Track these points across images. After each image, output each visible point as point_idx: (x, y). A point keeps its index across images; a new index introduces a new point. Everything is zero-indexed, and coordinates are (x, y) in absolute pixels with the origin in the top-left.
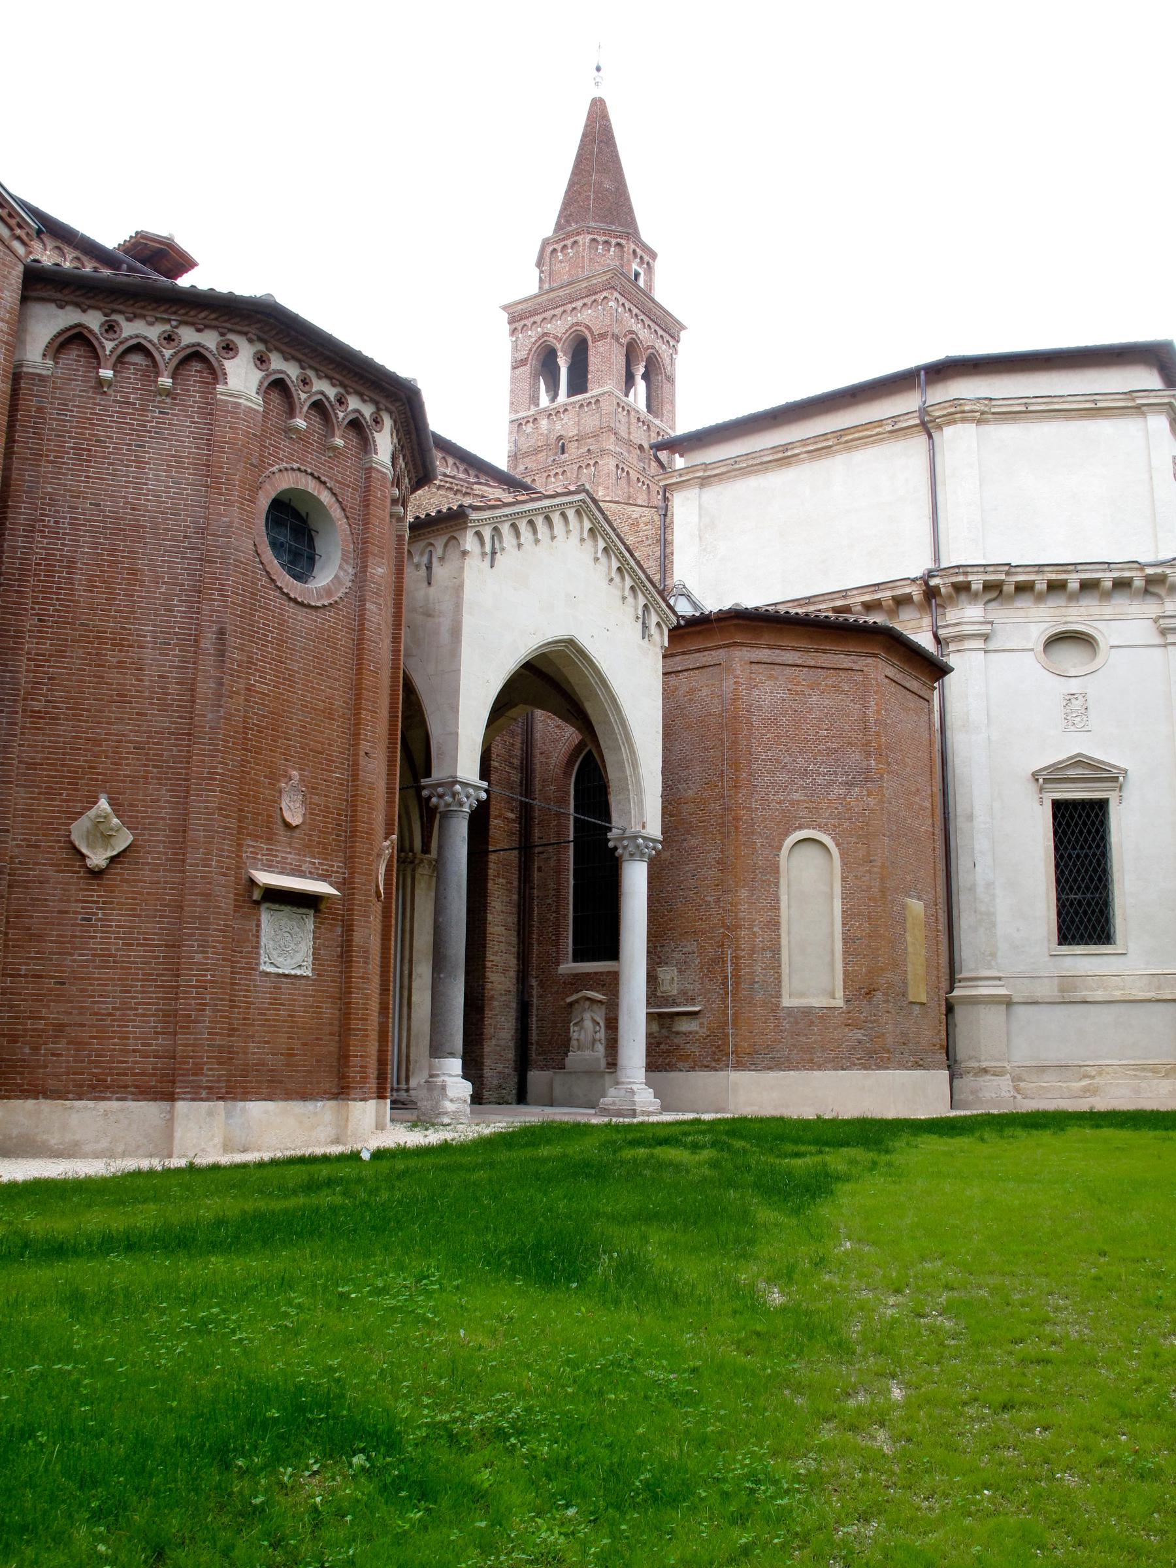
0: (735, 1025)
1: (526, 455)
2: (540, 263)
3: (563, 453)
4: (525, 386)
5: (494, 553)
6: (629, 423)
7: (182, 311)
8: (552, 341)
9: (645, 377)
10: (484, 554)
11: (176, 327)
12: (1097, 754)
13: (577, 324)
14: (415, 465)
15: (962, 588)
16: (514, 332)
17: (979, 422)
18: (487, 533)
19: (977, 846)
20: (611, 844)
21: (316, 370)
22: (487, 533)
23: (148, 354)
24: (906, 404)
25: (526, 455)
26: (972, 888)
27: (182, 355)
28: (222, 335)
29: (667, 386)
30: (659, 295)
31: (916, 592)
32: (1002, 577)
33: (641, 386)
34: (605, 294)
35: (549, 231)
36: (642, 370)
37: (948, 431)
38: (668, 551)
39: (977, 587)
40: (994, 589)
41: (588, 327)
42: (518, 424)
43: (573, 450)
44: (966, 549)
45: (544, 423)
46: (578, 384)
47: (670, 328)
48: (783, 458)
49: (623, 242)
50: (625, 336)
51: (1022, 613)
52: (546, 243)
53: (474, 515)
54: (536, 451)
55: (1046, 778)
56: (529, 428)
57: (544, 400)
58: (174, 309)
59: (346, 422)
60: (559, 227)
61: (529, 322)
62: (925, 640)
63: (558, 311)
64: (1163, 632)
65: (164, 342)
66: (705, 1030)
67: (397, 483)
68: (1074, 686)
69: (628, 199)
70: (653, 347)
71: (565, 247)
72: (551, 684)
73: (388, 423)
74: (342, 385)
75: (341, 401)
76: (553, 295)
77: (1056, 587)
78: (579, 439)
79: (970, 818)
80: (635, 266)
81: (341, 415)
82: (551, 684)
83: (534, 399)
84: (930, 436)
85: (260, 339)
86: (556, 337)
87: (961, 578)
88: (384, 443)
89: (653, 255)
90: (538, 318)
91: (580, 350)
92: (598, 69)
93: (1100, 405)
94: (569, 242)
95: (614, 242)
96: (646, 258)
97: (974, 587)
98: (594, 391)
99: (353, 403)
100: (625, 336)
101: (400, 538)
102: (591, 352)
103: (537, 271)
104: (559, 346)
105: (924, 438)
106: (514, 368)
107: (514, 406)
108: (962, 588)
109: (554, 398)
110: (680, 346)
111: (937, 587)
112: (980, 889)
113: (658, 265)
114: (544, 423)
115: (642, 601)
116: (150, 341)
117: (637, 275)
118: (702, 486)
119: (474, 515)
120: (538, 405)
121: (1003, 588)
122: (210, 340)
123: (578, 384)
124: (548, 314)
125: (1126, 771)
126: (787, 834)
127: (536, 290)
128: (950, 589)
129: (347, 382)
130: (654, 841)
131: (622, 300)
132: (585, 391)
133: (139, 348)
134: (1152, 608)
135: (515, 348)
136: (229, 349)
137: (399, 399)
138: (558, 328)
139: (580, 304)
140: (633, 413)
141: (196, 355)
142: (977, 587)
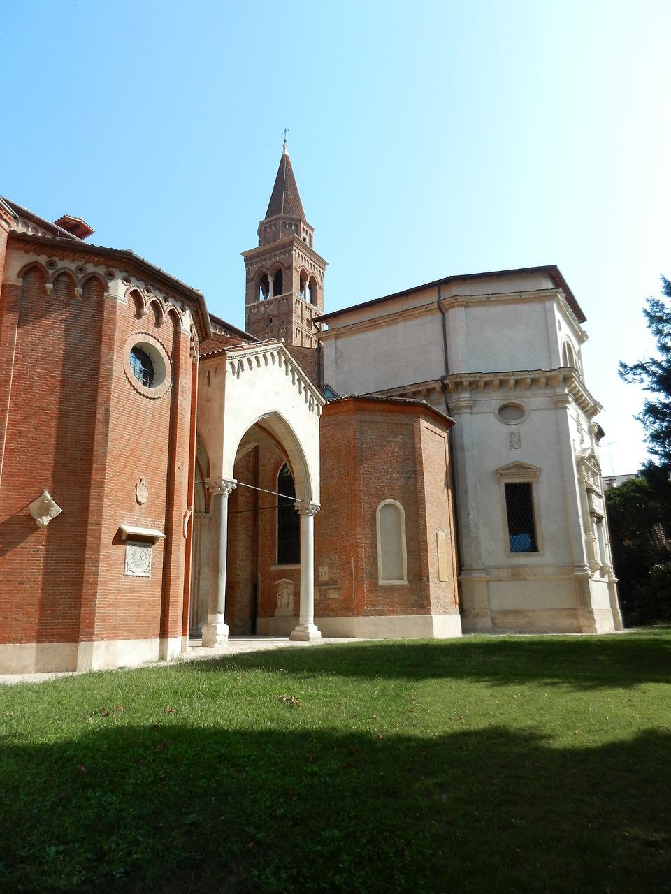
0: (356, 593)
1: (254, 323)
2: (259, 233)
3: (271, 322)
4: (253, 291)
5: (239, 372)
7: (87, 257)
8: (265, 271)
10: (233, 373)
11: (85, 264)
12: (526, 461)
14: (201, 331)
15: (458, 385)
16: (246, 266)
17: (466, 307)
18: (236, 362)
19: (470, 506)
20: (296, 509)
21: (153, 286)
22: (236, 362)
23: (69, 276)
24: (431, 298)
25: (254, 323)
26: (468, 526)
27: (87, 277)
28: (107, 268)
29: (319, 291)
30: (314, 248)
31: (438, 386)
32: (478, 379)
33: (307, 291)
34: (290, 248)
35: (262, 217)
36: (308, 284)
37: (451, 311)
38: (321, 368)
39: (466, 383)
40: (473, 386)
41: (282, 264)
42: (249, 310)
43: (276, 321)
44: (463, 365)
45: (262, 308)
46: (278, 290)
47: (322, 263)
48: (374, 324)
49: (298, 223)
50: (300, 267)
51: (488, 395)
52: (262, 224)
53: (229, 354)
54: (258, 322)
55: (499, 473)
56: (255, 311)
57: (262, 298)
58: (83, 256)
59: (168, 311)
60: (267, 216)
62: (441, 410)
64: (555, 403)
65: (79, 271)
66: (342, 596)
67: (192, 339)
68: (514, 428)
69: (300, 203)
70: (313, 273)
71: (270, 226)
73: (188, 312)
74: (166, 293)
77: (503, 383)
78: (279, 316)
79: (466, 492)
80: (303, 235)
81: (165, 307)
83: (258, 297)
84: (443, 313)
85: (126, 271)
86: (267, 268)
87: (458, 380)
88: (187, 319)
89: (312, 229)
90: (259, 259)
92: (285, 141)
93: (523, 297)
94: (273, 223)
95: (293, 223)
96: (309, 231)
97: (465, 383)
100: (300, 267)
101: (194, 365)
102: (284, 275)
103: (258, 236)
104: (268, 272)
105: (439, 315)
106: (247, 282)
107: (247, 302)
108: (458, 385)
109: (266, 298)
110: (325, 273)
111: (448, 385)
112: (472, 526)
113: (314, 235)
114: (262, 308)
115: (309, 394)
116: (72, 271)
117: (305, 239)
118: (336, 338)
119: (229, 354)
120: (259, 300)
121: (479, 384)
122: (101, 270)
123: (278, 290)
124: (263, 257)
125: (540, 469)
126: (379, 502)
128: (453, 386)
129: (168, 292)
130: (317, 506)
131: (298, 251)
132: (281, 294)
133: (64, 274)
134: (549, 391)
135: (248, 273)
136: (111, 276)
137: (193, 300)
138: (268, 263)
139: (278, 252)
140: (303, 304)
141: (94, 277)
142: (466, 383)
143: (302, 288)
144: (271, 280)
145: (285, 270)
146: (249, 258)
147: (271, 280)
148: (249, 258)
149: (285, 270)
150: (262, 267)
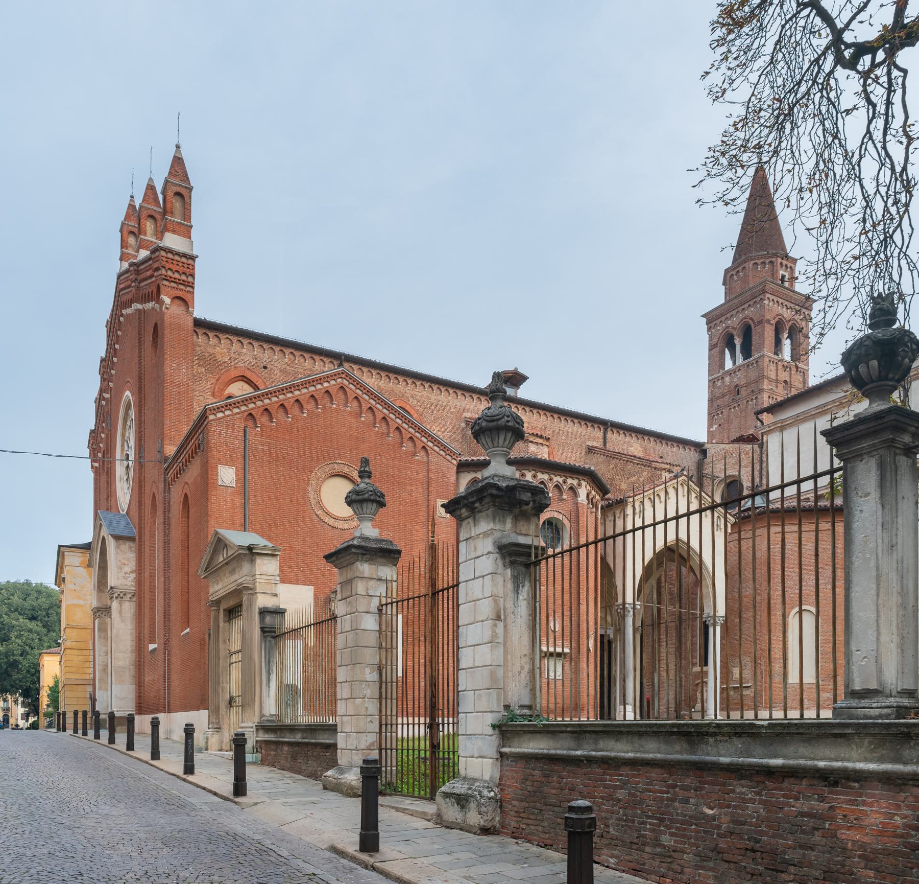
6: (777, 370)
9: (789, 337)
13: (745, 318)
36: (786, 335)
41: (751, 319)
61: (718, 322)
63: (734, 312)
72: (675, 559)
75: (565, 482)
76: (731, 303)
82: (675, 559)
86: (733, 328)
90: (723, 319)
91: (747, 333)
98: (756, 355)
99: (570, 481)
102: (754, 332)
104: (735, 333)
123: (747, 353)
127: (723, 301)
138: (735, 322)
143: (778, 343)
144: (738, 342)
145: (755, 326)
146: (712, 318)
147: (738, 342)
148: (712, 318)
149: (755, 326)
150: (728, 327)
